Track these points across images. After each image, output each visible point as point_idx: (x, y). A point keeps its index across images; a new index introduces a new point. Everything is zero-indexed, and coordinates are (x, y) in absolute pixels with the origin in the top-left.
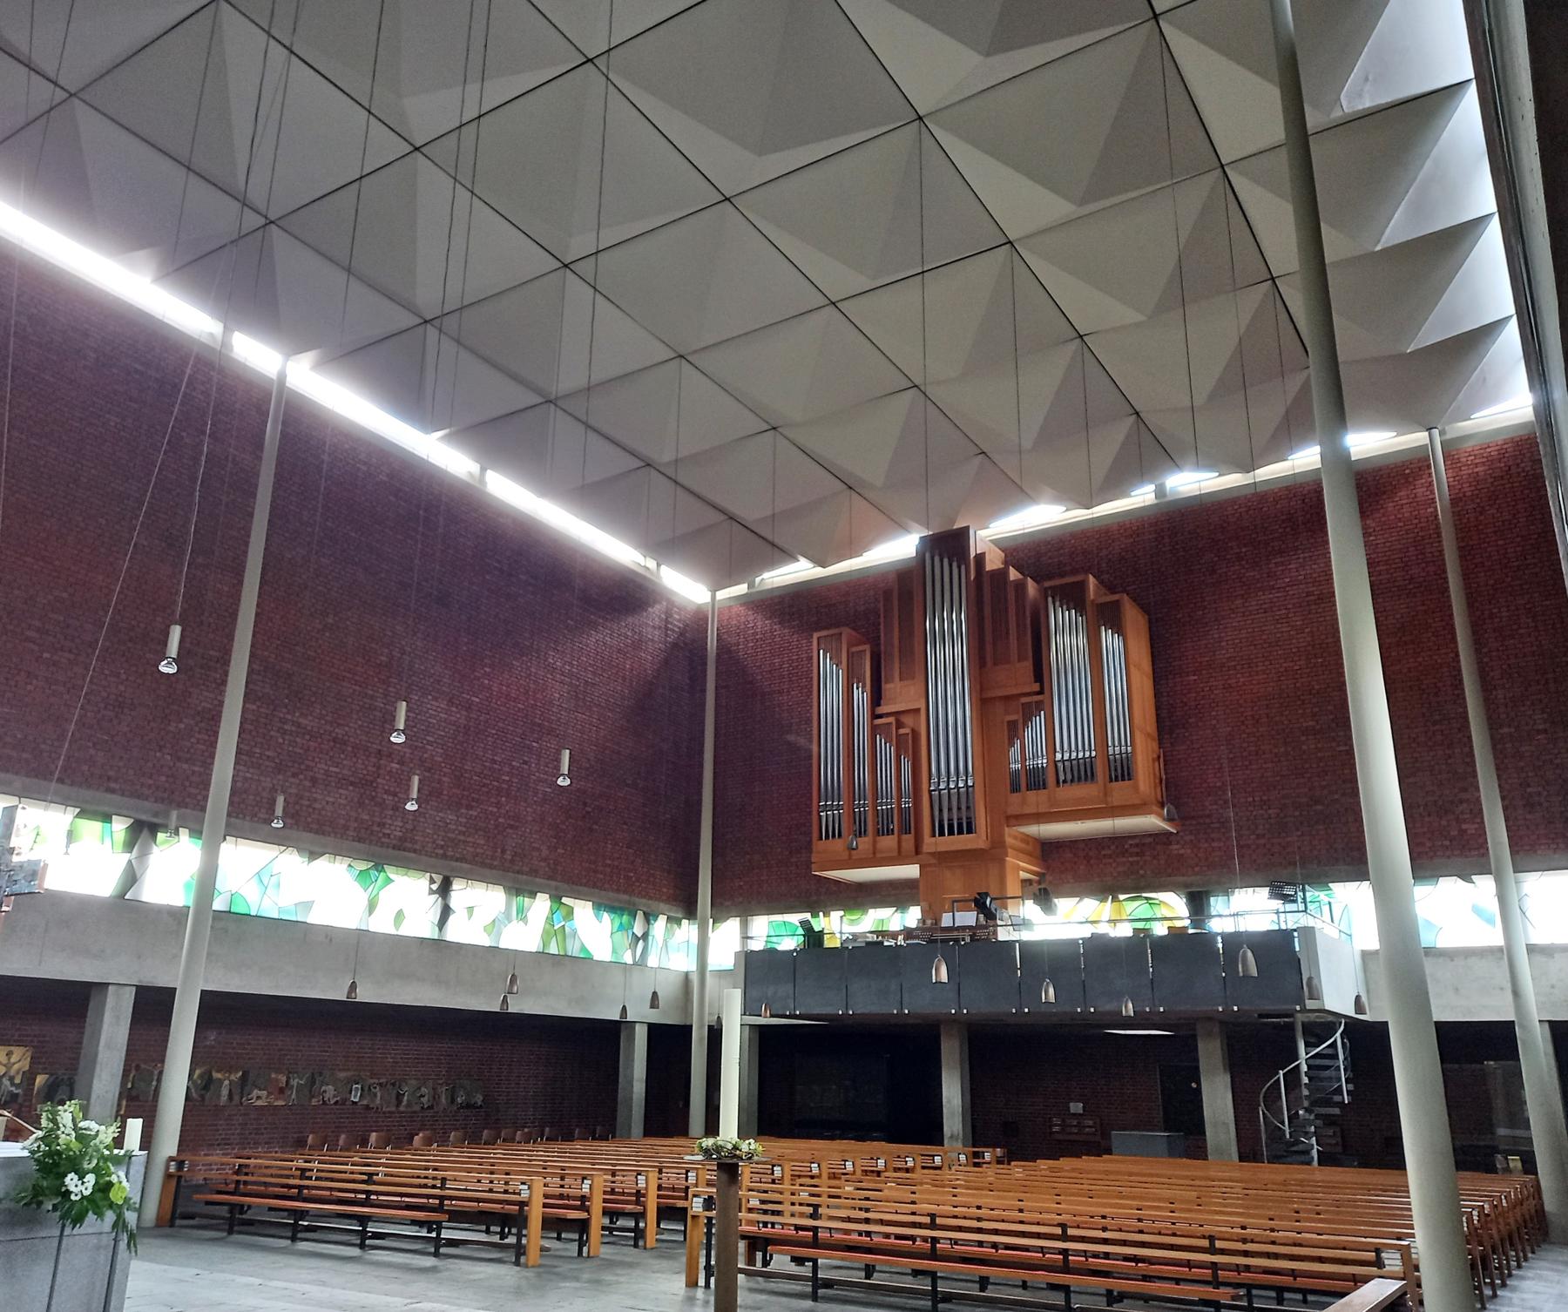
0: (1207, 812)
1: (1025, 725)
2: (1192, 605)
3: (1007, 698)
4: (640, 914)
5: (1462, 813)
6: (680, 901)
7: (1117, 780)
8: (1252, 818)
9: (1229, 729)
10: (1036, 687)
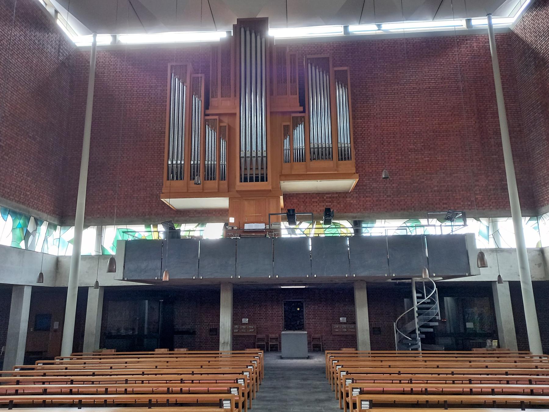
0: (364, 184)
1: (294, 129)
2: (361, 87)
3: (283, 113)
4: (32, 219)
5: (476, 191)
6: (57, 215)
7: (342, 160)
8: (385, 188)
9: (376, 146)
10: (301, 109)
